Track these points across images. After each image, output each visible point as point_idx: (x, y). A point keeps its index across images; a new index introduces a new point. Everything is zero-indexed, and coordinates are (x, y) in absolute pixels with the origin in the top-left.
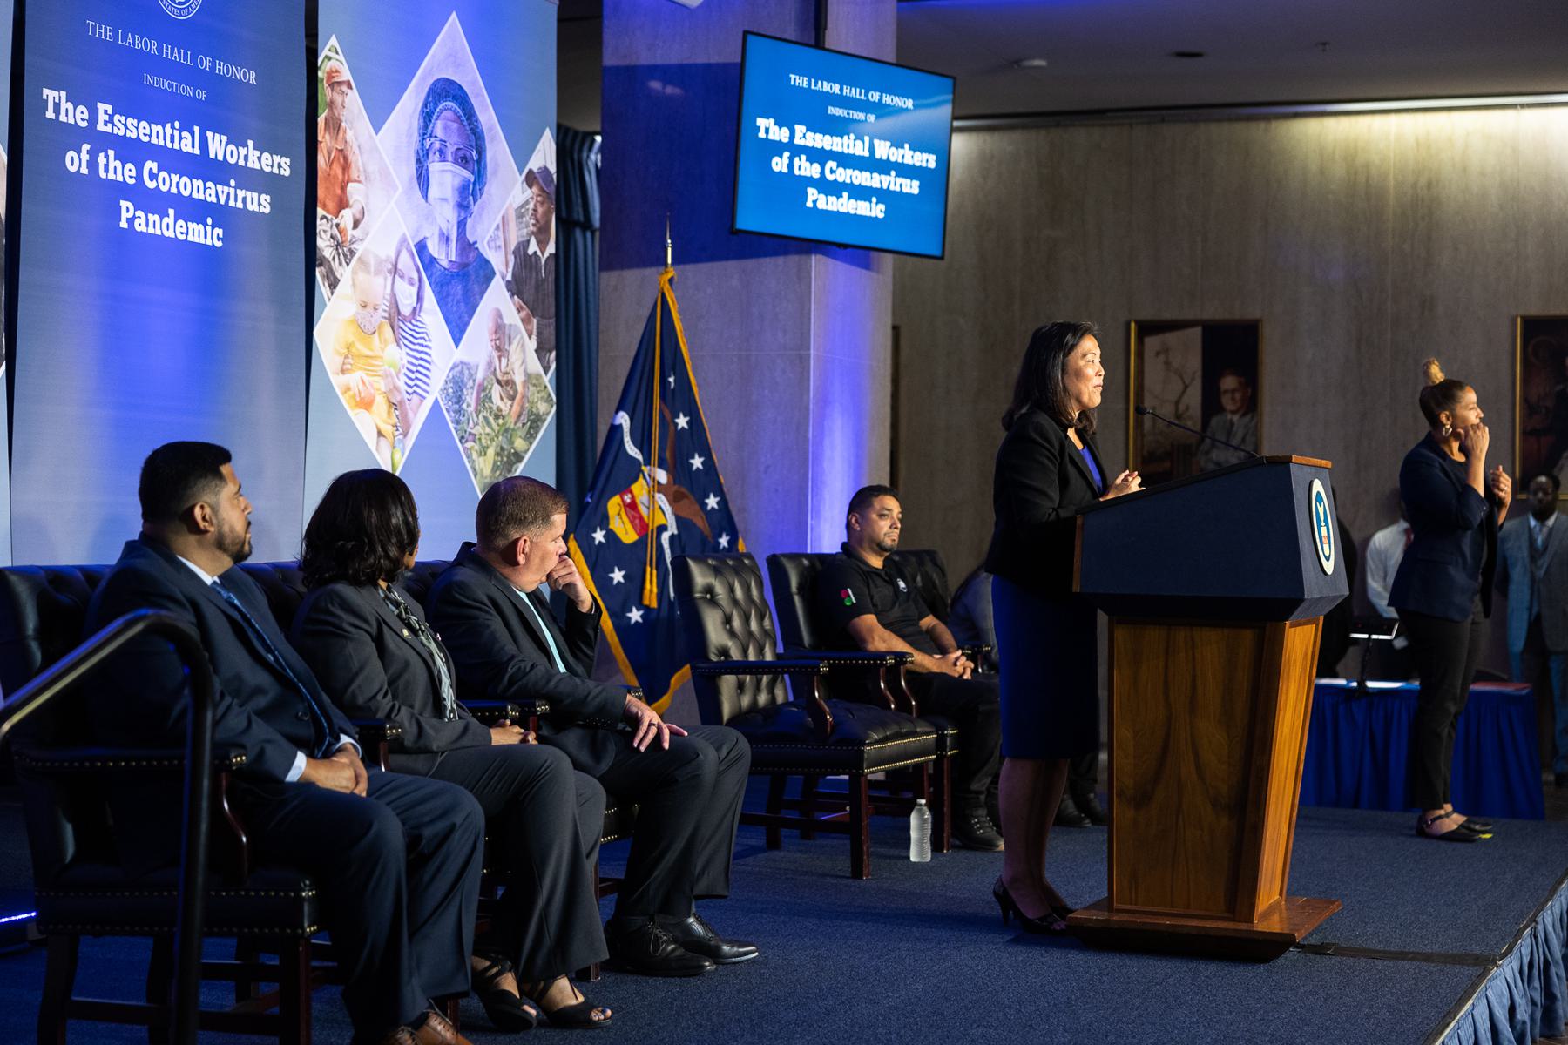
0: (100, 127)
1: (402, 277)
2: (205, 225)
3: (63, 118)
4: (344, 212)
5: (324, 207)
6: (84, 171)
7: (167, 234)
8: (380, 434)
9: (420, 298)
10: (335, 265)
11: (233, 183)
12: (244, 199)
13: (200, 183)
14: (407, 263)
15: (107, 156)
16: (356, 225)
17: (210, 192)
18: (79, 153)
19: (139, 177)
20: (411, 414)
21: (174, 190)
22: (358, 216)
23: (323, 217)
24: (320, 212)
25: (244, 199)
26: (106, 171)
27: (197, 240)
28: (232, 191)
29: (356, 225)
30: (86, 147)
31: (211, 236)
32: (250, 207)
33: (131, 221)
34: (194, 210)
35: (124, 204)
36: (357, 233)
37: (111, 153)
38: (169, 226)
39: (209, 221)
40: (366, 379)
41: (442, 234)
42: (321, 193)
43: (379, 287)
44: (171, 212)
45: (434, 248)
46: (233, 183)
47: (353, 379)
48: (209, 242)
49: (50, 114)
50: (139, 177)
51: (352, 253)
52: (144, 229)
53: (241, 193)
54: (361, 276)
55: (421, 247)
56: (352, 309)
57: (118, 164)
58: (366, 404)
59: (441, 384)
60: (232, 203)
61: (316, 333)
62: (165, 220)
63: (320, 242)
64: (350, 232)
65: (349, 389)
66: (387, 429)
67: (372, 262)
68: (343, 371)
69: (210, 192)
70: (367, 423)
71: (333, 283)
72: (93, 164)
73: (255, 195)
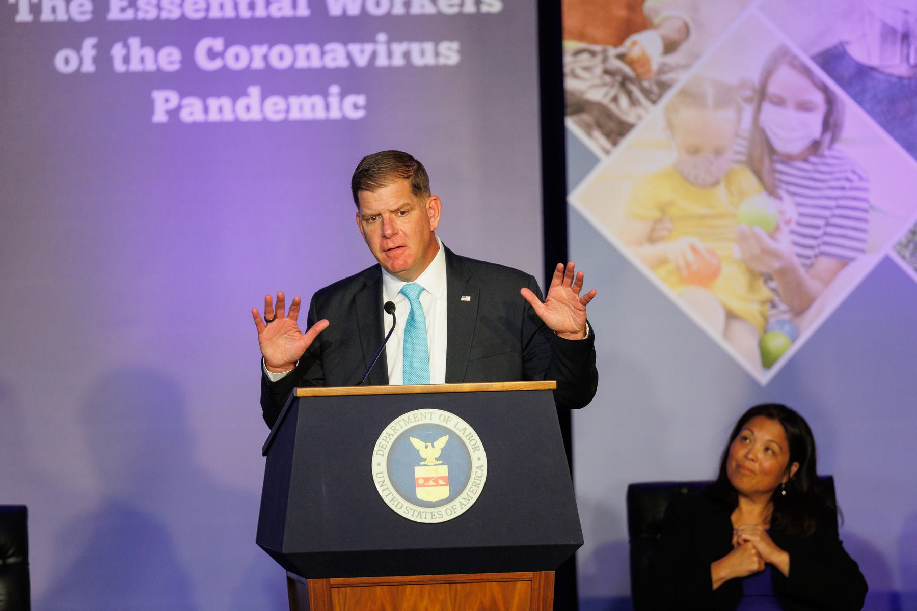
0: (114, 14)
1: (780, 102)
2: (325, 95)
3: (46, 16)
4: (636, 37)
5: (581, 37)
6: (89, 67)
7: (244, 116)
8: (731, 316)
9: (831, 124)
10: (624, 109)
11: (382, 37)
12: (407, 55)
13: (314, 49)
14: (785, 80)
15: (126, 46)
16: (670, 47)
17: (336, 56)
18: (78, 48)
19: (188, 59)
20: (812, 284)
21: (258, 64)
22: (674, 36)
23: (577, 53)
24: (570, 45)
25: (407, 55)
26: (127, 60)
27: (308, 115)
28: (382, 49)
29: (670, 47)
30: (89, 46)
31: (351, 107)
32: (417, 60)
33: (174, 114)
34: (313, 82)
35: (159, 96)
36: (671, 59)
37: (134, 42)
38: (253, 107)
39: (335, 89)
40: (700, 246)
41: (888, 33)
42: (571, 19)
43: (730, 125)
44: (255, 92)
45: (865, 51)
46: (382, 37)
47: (677, 247)
48: (335, 114)
49: (23, 16)
50: (188, 59)
51: (664, 86)
52: (199, 116)
53: (398, 49)
54: (687, 115)
55: (832, 59)
56: (669, 157)
57: (148, 52)
58: (704, 276)
59: (902, 233)
60: (382, 61)
61: (576, 199)
62: (242, 103)
63: (570, 84)
64: (656, 58)
65: (662, 262)
66: (749, 307)
67: (710, 92)
68: (652, 239)
69: (336, 56)
70: (702, 308)
71: (616, 130)
72: (103, 58)
73: (429, 47)
